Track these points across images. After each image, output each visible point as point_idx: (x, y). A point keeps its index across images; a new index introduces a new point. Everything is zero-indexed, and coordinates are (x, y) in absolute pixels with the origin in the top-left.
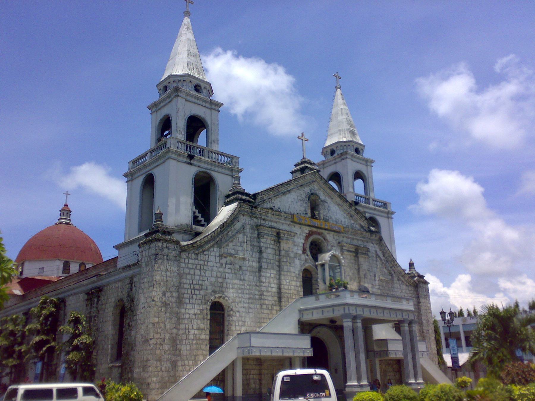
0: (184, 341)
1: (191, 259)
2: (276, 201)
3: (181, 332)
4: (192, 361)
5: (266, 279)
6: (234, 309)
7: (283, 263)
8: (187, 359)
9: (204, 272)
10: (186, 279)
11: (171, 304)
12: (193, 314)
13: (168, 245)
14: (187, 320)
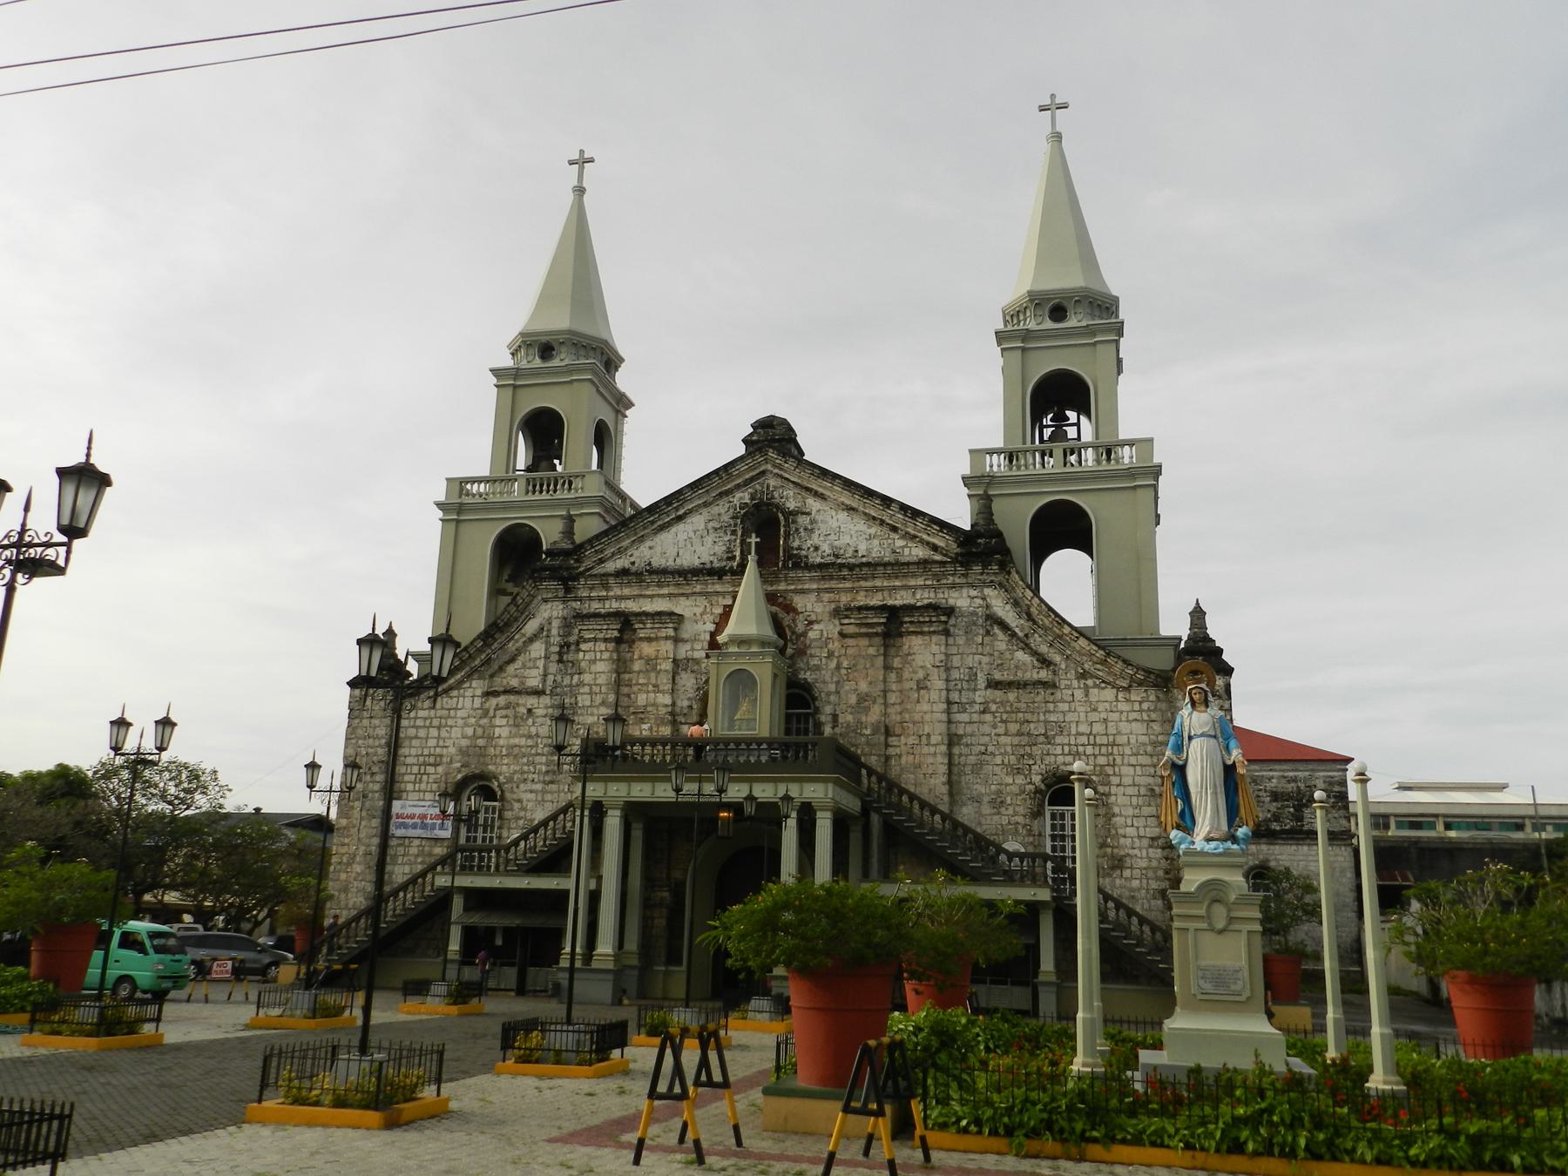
0: (401, 858)
1: (423, 709)
2: (640, 550)
10: (411, 747)
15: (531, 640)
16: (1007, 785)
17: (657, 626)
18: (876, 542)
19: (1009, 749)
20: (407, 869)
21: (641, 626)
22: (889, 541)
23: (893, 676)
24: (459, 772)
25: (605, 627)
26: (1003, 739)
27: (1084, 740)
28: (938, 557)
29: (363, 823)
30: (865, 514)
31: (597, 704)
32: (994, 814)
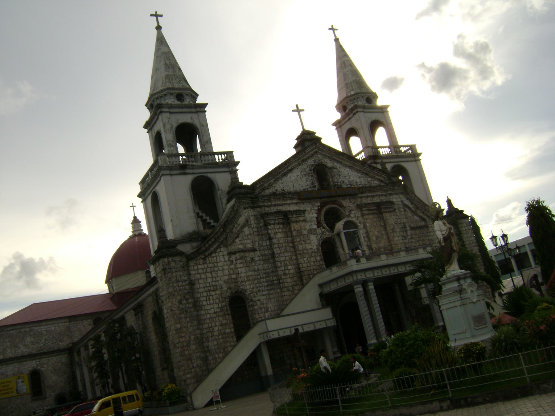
0: (210, 338)
1: (200, 264)
2: (277, 184)
3: (205, 331)
4: (222, 353)
5: (281, 263)
6: (253, 298)
7: (296, 244)
8: (217, 353)
9: (215, 273)
10: (199, 284)
11: (188, 310)
12: (213, 313)
13: (173, 258)
14: (208, 320)
15: (244, 226)
17: (298, 216)
20: (215, 343)
21: (292, 216)
24: (227, 292)
25: (277, 218)
28: (382, 184)
29: (189, 324)
31: (283, 251)
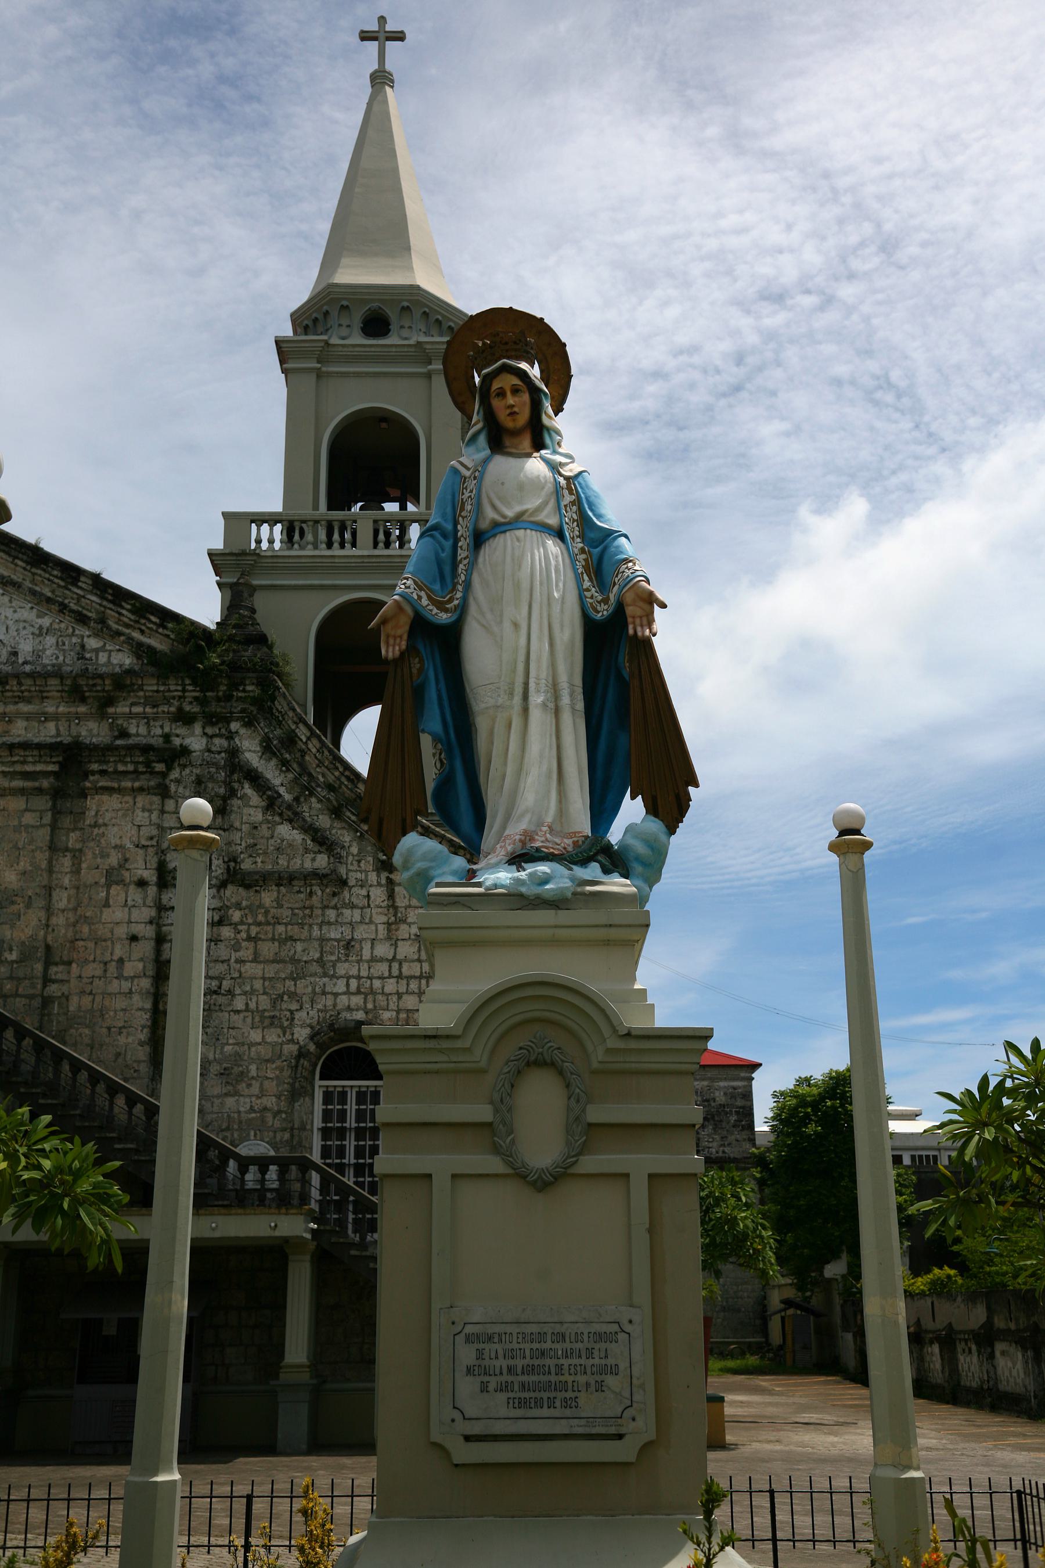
16: (251, 1045)
18: (50, 640)
19: (258, 985)
22: (74, 640)
23: (66, 862)
26: (250, 969)
27: (382, 968)
30: (33, 593)
32: (226, 1095)
